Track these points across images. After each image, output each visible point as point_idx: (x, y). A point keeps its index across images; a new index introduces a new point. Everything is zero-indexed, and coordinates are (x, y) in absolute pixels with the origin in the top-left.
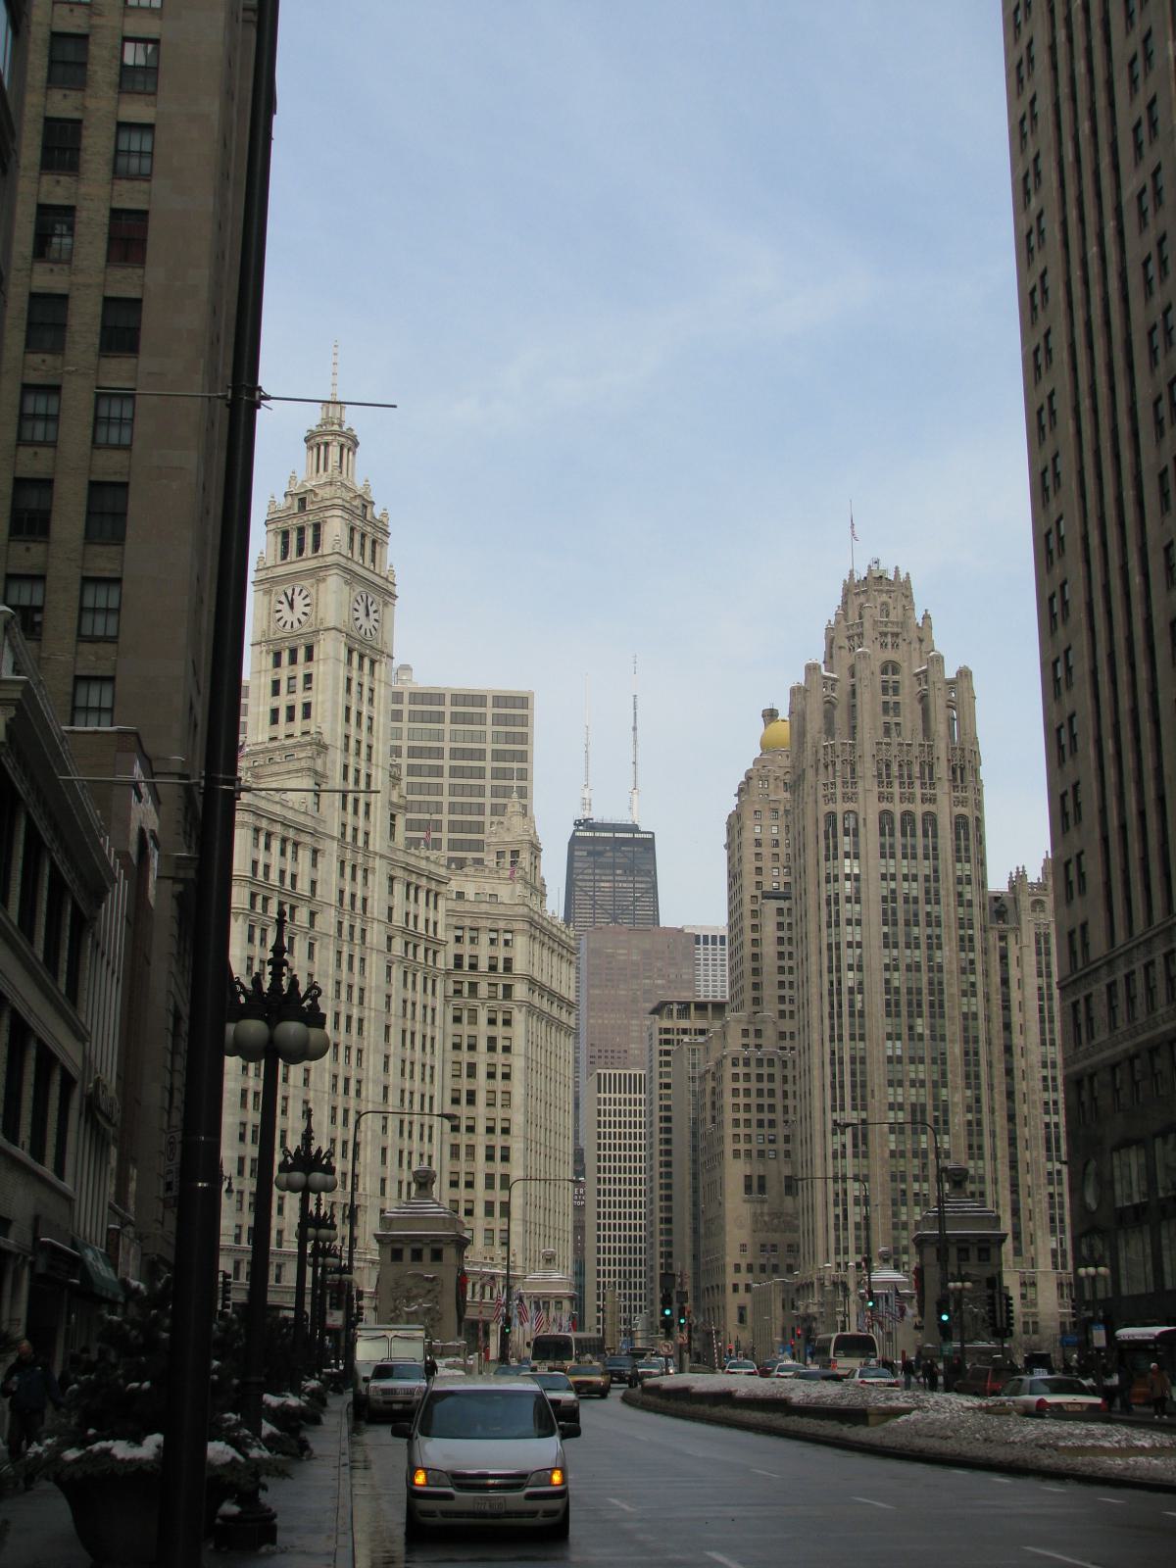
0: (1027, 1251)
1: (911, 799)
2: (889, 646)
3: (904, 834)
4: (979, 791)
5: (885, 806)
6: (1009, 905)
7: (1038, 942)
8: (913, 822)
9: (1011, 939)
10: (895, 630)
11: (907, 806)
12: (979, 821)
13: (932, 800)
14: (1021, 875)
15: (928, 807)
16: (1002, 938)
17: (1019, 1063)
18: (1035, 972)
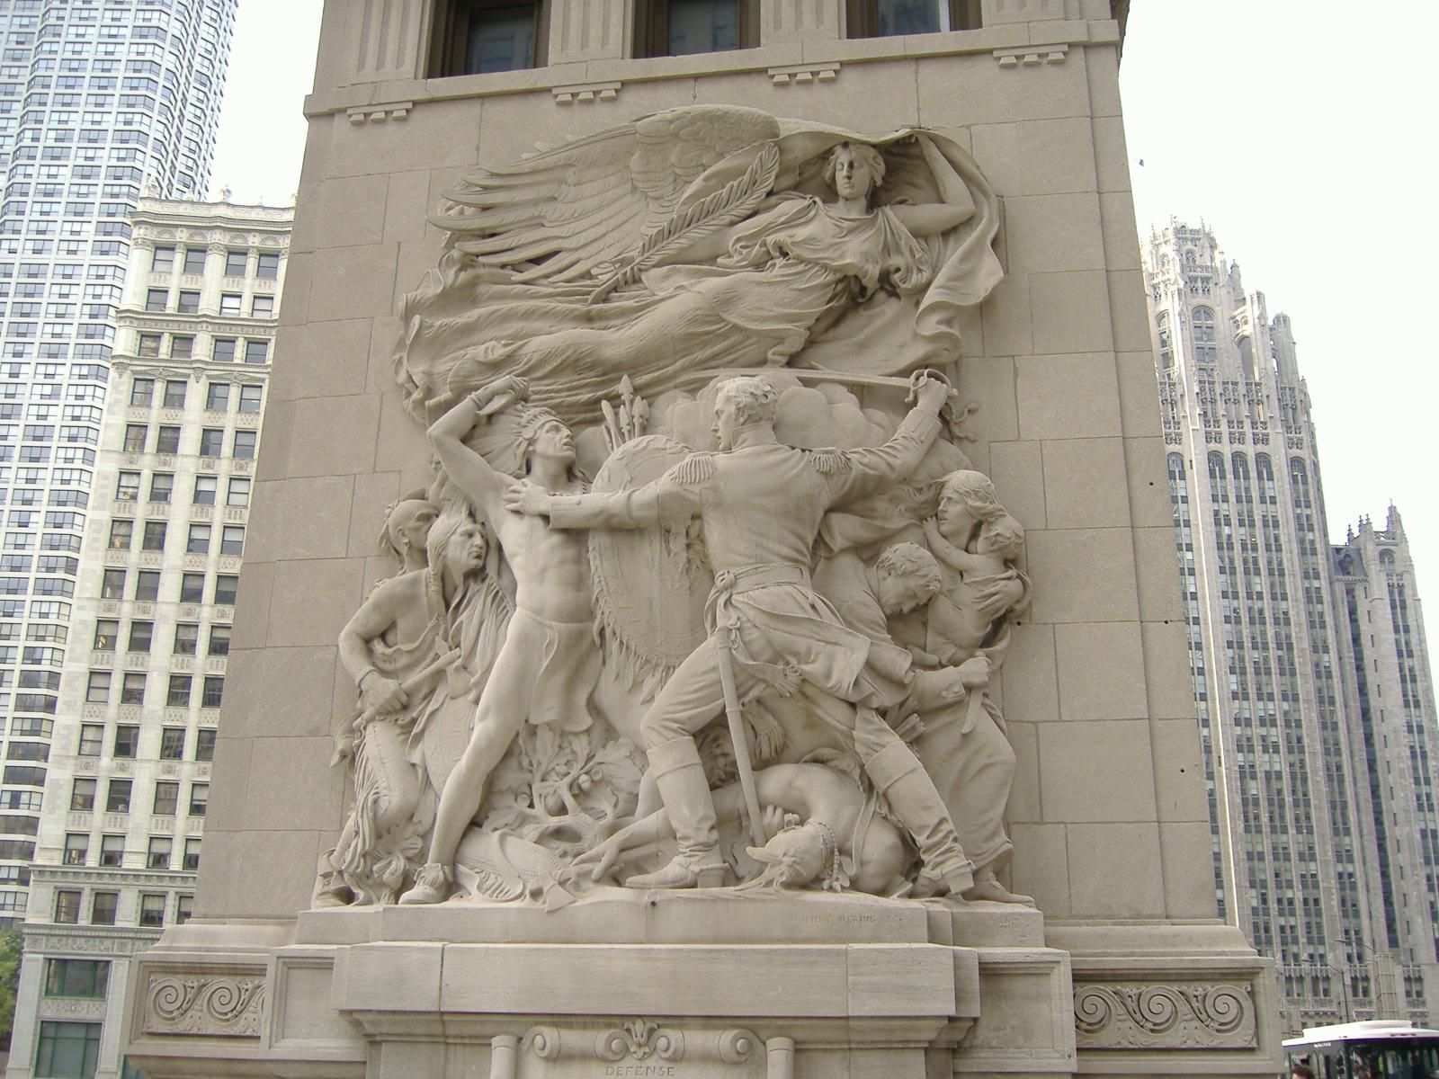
0: (1404, 941)
1: (1241, 440)
2: (1200, 291)
3: (1236, 477)
4: (1312, 435)
5: (1213, 446)
6: (1353, 555)
7: (1391, 593)
8: (1245, 463)
9: (1359, 593)
10: (1205, 274)
11: (1237, 447)
12: (1316, 466)
13: (1265, 440)
14: (1364, 526)
15: (1261, 448)
16: (1350, 592)
17: (1378, 729)
18: (1391, 627)
